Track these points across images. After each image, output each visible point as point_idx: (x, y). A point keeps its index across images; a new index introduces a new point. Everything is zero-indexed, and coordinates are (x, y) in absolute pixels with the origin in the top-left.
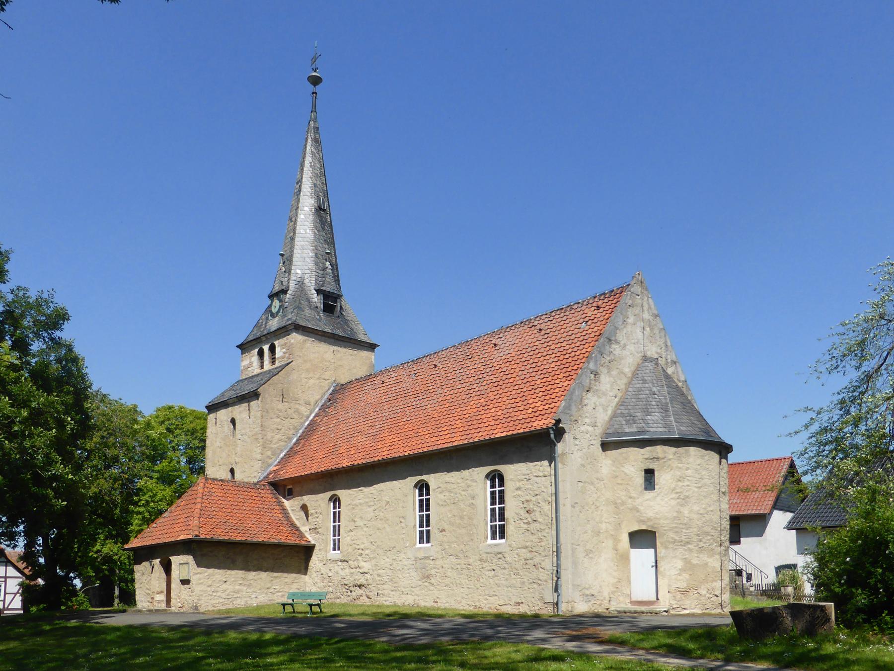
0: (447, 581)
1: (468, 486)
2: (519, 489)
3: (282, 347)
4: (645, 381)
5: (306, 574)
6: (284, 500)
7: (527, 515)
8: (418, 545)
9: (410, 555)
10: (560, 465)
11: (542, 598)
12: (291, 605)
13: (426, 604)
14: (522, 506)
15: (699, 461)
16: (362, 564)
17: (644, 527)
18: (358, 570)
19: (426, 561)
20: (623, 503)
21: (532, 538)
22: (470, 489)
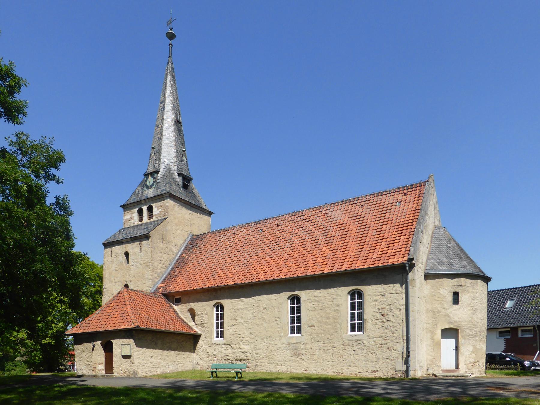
0: (315, 357)
1: (334, 299)
2: (376, 301)
3: (159, 208)
4: (440, 240)
5: (194, 352)
6: (173, 305)
7: (382, 317)
8: (290, 335)
9: (284, 341)
10: (410, 287)
11: (394, 368)
12: (216, 372)
13: (297, 371)
14: (378, 311)
15: (481, 289)
16: (242, 346)
17: (452, 326)
18: (239, 350)
19: (297, 345)
20: (439, 312)
21: (386, 331)
22: (335, 300)
